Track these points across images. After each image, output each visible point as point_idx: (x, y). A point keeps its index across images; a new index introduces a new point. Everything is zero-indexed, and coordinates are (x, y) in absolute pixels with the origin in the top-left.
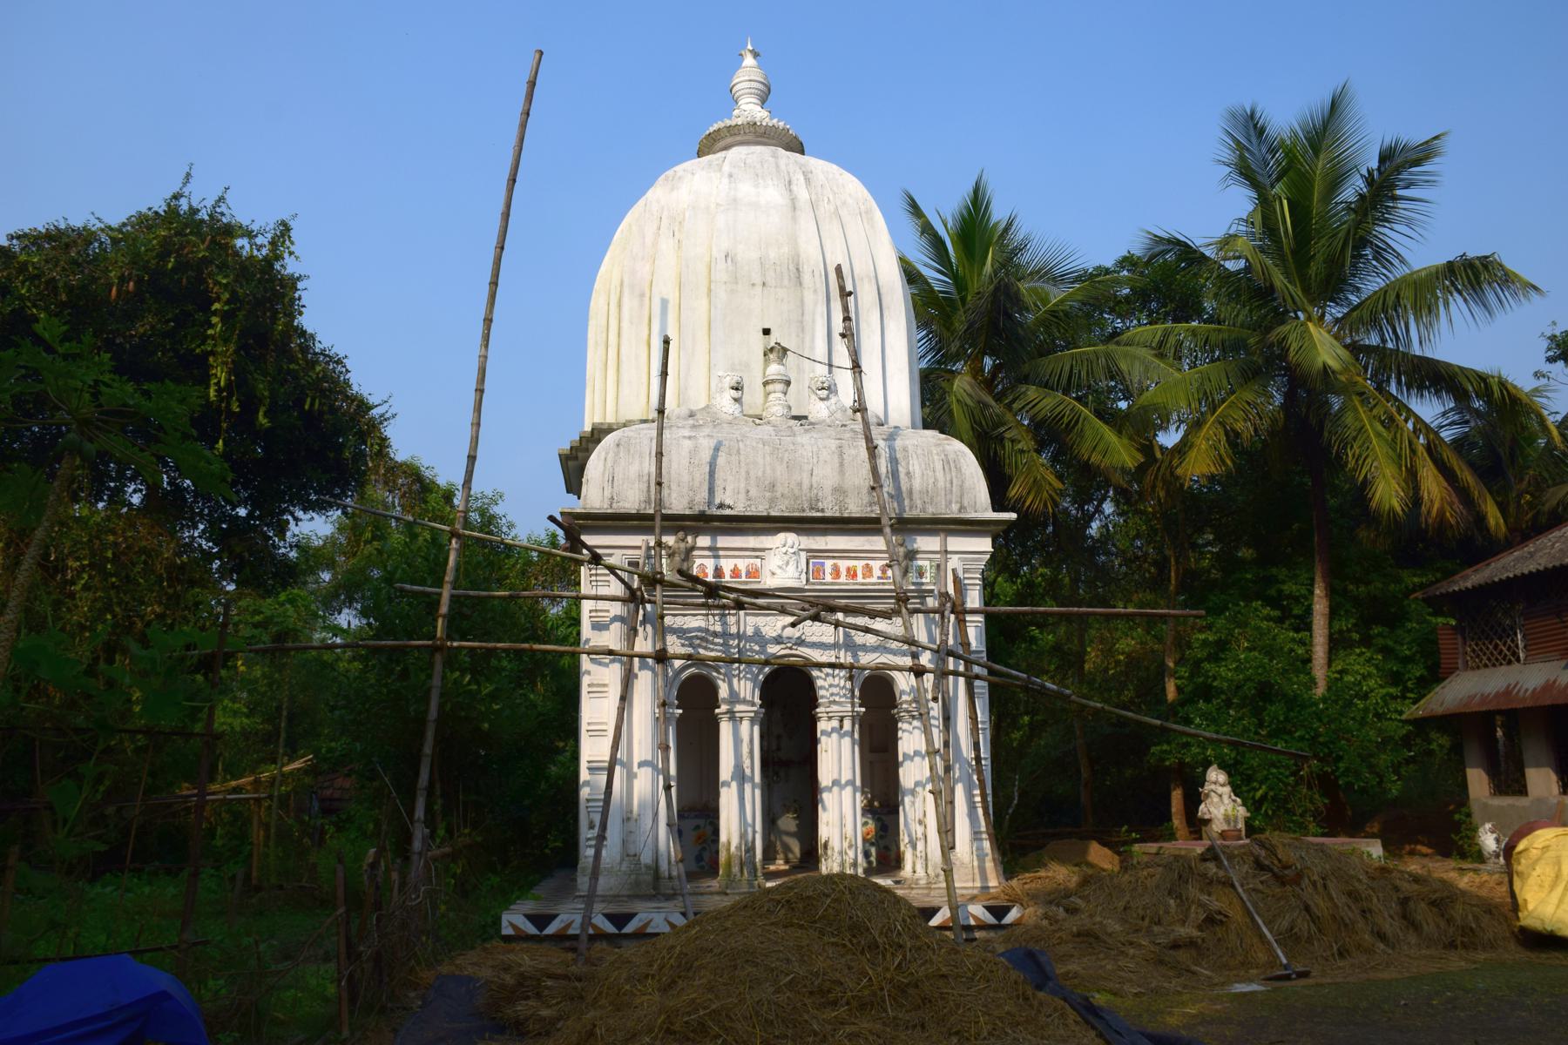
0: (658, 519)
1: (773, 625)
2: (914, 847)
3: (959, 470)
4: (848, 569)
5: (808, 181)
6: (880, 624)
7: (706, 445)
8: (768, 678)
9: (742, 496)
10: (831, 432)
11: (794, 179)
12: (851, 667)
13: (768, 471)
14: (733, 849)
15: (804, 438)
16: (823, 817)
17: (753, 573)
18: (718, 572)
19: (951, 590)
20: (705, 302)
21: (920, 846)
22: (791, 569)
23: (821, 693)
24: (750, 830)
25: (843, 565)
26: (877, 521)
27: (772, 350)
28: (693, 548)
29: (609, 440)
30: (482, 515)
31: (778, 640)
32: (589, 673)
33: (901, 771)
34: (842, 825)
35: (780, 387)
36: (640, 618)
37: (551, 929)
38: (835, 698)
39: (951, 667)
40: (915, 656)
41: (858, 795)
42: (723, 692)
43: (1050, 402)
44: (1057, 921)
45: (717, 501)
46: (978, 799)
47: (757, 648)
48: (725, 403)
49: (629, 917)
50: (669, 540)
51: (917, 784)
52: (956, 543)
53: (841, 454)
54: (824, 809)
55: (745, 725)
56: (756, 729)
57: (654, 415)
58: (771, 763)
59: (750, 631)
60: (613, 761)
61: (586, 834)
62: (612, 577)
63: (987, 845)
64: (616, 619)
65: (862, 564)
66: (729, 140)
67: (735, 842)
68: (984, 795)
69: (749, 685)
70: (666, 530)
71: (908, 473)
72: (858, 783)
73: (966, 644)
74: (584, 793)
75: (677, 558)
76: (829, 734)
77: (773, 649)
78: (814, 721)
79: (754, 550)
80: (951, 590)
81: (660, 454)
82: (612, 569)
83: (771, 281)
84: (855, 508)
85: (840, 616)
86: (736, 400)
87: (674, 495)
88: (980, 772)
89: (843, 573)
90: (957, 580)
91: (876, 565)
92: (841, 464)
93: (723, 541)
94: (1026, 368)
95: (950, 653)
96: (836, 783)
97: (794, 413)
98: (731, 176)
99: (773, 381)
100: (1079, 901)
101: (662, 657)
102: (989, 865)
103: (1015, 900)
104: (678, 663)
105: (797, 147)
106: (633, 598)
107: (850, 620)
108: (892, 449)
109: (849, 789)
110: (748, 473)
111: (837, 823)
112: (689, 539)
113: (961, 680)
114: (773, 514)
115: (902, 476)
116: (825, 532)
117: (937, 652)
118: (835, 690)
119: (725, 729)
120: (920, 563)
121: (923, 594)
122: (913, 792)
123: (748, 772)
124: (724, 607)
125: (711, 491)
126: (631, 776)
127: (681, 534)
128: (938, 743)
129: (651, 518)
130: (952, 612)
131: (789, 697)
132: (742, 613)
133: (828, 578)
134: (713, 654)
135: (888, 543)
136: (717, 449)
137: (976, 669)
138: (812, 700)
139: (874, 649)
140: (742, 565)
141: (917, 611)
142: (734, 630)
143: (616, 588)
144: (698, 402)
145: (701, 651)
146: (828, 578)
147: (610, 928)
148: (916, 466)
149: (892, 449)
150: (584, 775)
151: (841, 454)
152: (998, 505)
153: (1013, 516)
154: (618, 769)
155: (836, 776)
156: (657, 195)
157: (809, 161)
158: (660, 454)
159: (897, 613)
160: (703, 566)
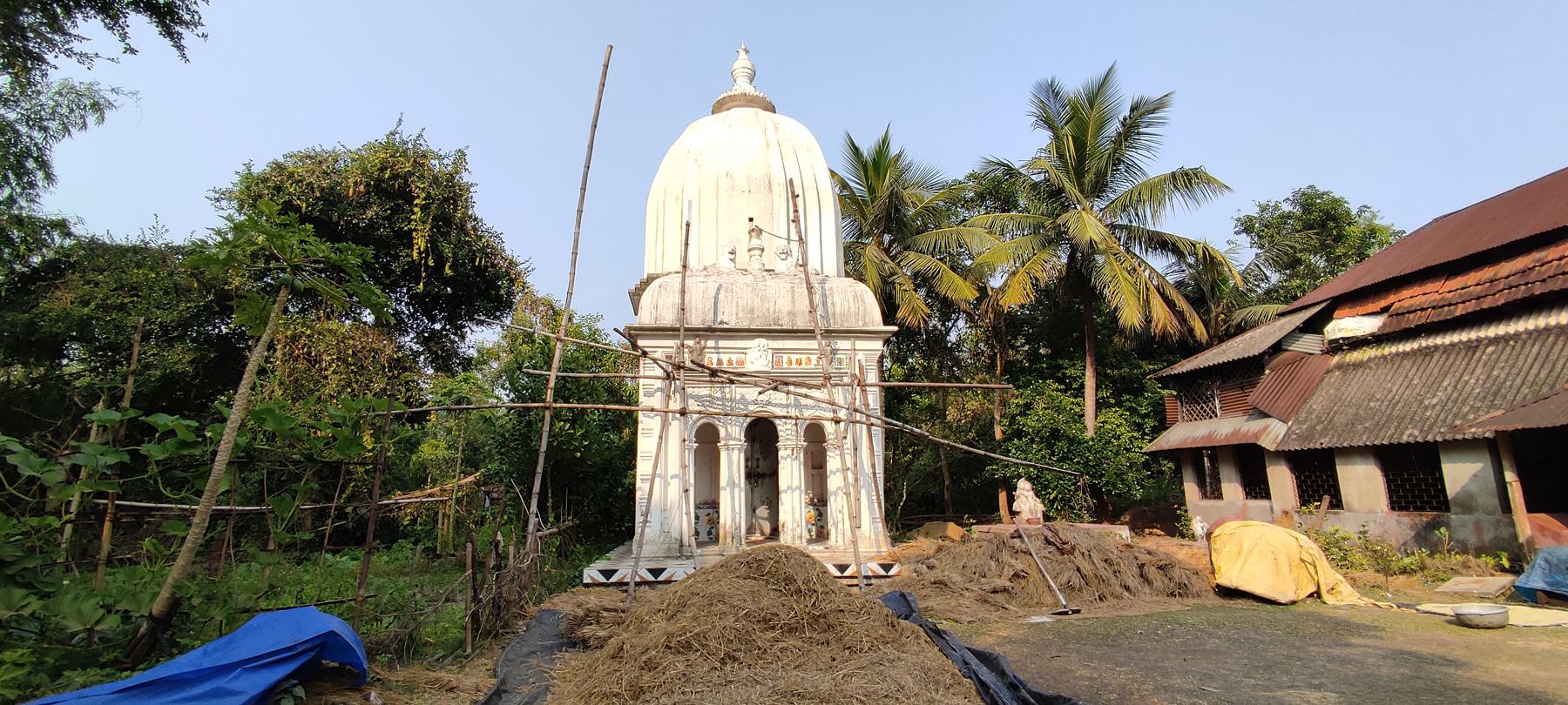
1: (751, 393)
6: (815, 393)
7: (713, 287)
17: (741, 363)
18: (720, 362)
25: (794, 357)
29: (656, 283)
31: (755, 402)
37: (614, 579)
38: (789, 441)
42: (722, 433)
48: (725, 263)
49: (662, 570)
50: (690, 343)
52: (860, 344)
58: (750, 475)
61: (639, 519)
63: (880, 525)
64: (658, 390)
65: (803, 356)
67: (729, 523)
70: (686, 337)
74: (638, 494)
77: (752, 408)
78: (777, 450)
81: (683, 292)
82: (655, 360)
84: (801, 324)
85: (792, 388)
91: (814, 358)
93: (722, 343)
94: (909, 241)
95: (856, 410)
96: (789, 488)
101: (683, 413)
102: (881, 538)
104: (695, 416)
106: (668, 377)
107: (799, 390)
116: (783, 338)
119: (723, 455)
121: (841, 375)
122: (836, 494)
125: (715, 313)
126: (666, 484)
128: (849, 463)
131: (762, 434)
138: (776, 438)
140: (734, 357)
147: (651, 578)
148: (837, 299)
152: (886, 323)
153: (896, 328)
154: (657, 480)
158: (683, 292)
160: (711, 359)
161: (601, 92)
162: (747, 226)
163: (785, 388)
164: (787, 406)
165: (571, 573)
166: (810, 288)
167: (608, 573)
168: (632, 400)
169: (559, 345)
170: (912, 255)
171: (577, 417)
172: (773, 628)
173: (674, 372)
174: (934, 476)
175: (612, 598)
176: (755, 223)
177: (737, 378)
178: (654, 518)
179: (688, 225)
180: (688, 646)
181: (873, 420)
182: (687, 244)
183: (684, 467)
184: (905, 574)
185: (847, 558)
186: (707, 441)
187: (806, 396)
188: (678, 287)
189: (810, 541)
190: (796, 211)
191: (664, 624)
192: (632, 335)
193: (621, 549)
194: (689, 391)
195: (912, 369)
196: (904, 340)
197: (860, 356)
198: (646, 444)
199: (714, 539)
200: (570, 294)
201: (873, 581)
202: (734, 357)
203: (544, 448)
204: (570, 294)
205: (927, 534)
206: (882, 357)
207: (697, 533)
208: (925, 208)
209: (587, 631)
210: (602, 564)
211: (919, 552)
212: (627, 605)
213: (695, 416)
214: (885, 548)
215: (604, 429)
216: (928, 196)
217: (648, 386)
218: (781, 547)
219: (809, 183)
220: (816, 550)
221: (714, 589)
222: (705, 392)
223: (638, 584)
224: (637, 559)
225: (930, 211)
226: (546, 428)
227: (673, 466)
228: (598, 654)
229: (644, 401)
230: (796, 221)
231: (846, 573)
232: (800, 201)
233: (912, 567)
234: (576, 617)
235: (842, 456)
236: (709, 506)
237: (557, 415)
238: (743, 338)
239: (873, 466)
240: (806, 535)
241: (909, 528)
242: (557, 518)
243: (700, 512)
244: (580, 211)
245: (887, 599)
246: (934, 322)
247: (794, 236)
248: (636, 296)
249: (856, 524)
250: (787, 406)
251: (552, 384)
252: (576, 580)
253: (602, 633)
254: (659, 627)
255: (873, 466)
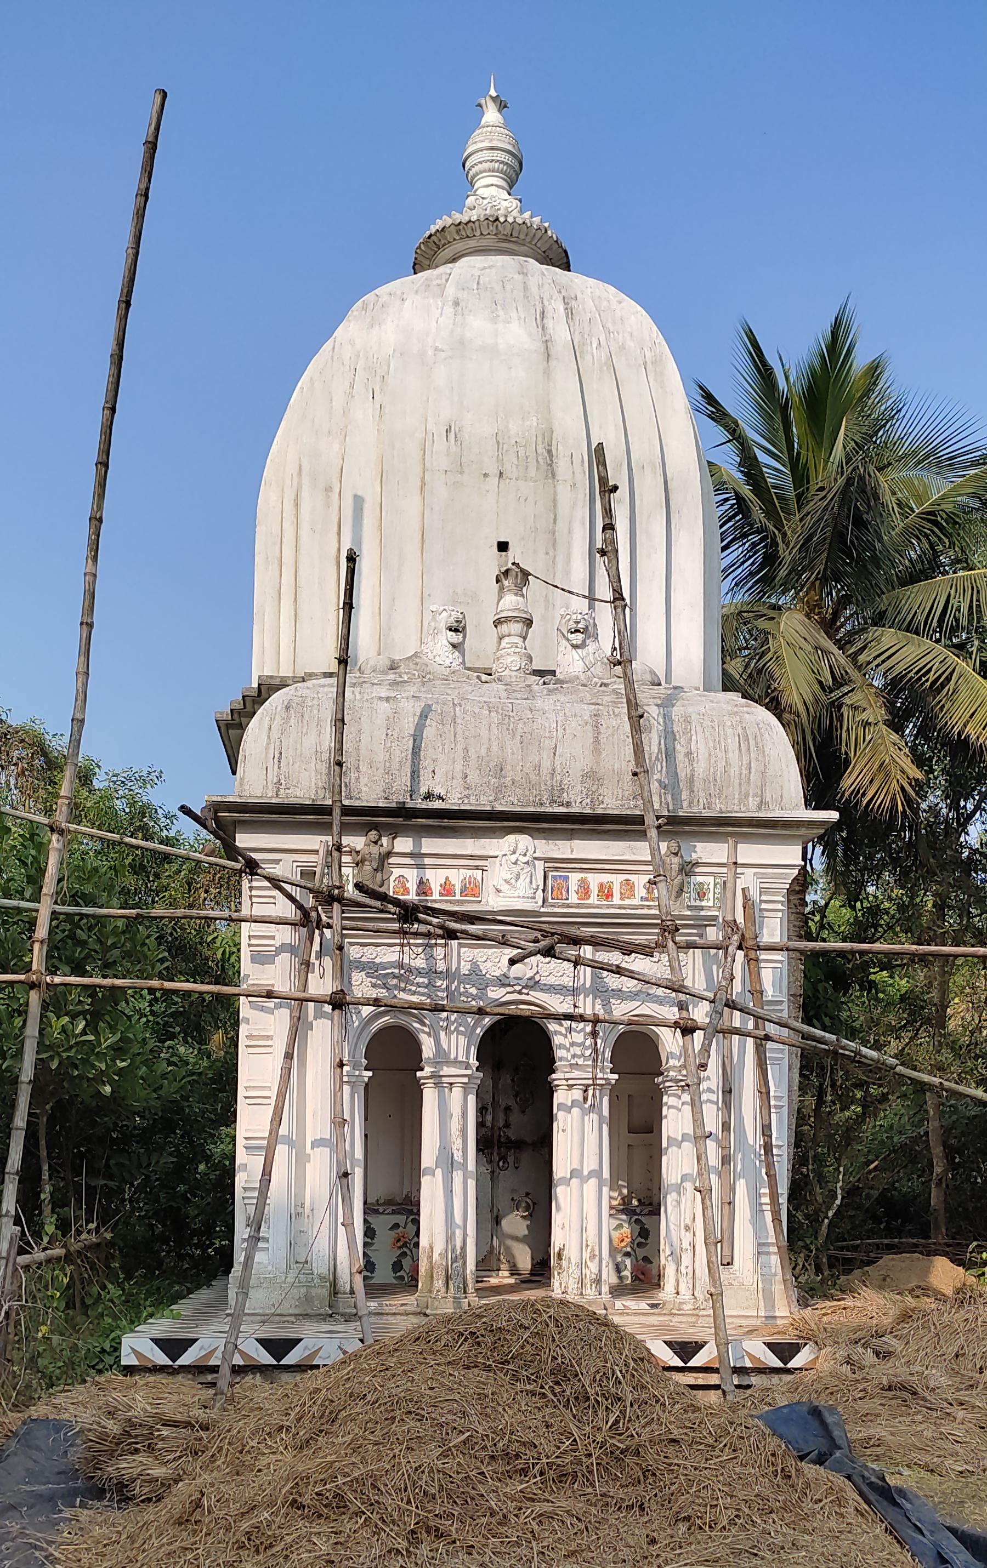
0: (337, 812)
1: (494, 961)
2: (678, 1263)
3: (761, 749)
4: (601, 886)
5: (570, 313)
6: (638, 963)
7: (410, 710)
8: (490, 1033)
9: (458, 783)
10: (585, 693)
11: (549, 310)
12: (596, 1021)
13: (495, 748)
14: (436, 1256)
15: (548, 703)
16: (557, 1219)
17: (471, 889)
19: (740, 919)
20: (417, 499)
21: (686, 1259)
22: (523, 883)
23: (559, 1053)
24: (458, 1233)
25: (594, 880)
26: (640, 820)
27: (506, 573)
28: (389, 854)
29: (276, 700)
30: (132, 804)
31: (503, 981)
32: (247, 1021)
33: (664, 1159)
34: (583, 1229)
35: (517, 627)
36: (316, 947)
37: (186, 1359)
38: (577, 1063)
39: (737, 1023)
40: (682, 1007)
41: (605, 1190)
42: (428, 1049)
43: (910, 652)
44: (862, 1368)
45: (423, 790)
46: (766, 1200)
47: (474, 991)
48: (440, 651)
50: (357, 842)
51: (684, 1178)
52: (749, 852)
53: (597, 726)
54: (558, 1209)
55: (457, 1092)
56: (472, 1099)
57: (334, 667)
58: (488, 1144)
59: (465, 970)
60: (274, 1138)
61: (241, 1232)
62: (276, 893)
63: (775, 1260)
64: (283, 948)
65: (616, 879)
66: (459, 246)
67: (439, 1248)
68: (774, 1195)
69: (463, 1040)
70: (346, 828)
71: (689, 754)
72: (606, 1174)
73: (757, 992)
75: (367, 867)
76: (568, 1110)
77: (496, 993)
79: (472, 857)
80: (740, 919)
81: (340, 722)
82: (275, 883)
83: (510, 470)
84: (612, 804)
85: (587, 951)
86: (454, 646)
87: (364, 780)
88: (770, 1166)
89: (594, 890)
90: (748, 904)
91: (640, 881)
92: (596, 740)
93: (430, 845)
94: (883, 602)
95: (731, 1005)
96: (574, 1173)
97: (535, 667)
98: (456, 304)
99: (507, 620)
100: (894, 1342)
101: (339, 1002)
103: (809, 1337)
105: (560, 259)
106: (306, 921)
107: (604, 956)
108: (667, 718)
109: (593, 1182)
110: (466, 750)
111: (576, 1226)
112: (384, 840)
113: (750, 1041)
114: (499, 808)
115: (680, 757)
116: (571, 835)
117: (712, 1002)
118: (578, 1051)
119: (430, 1096)
120: (699, 879)
121: (702, 923)
122: (679, 1189)
123: (458, 1156)
124: (428, 935)
125: (415, 774)
126: (302, 1159)
127: (373, 834)
128: (712, 1122)
129: (326, 811)
130: (740, 948)
131: (516, 1054)
132: (454, 943)
133: (574, 898)
134: (415, 999)
135: (654, 851)
136: (424, 716)
137: (772, 1029)
139: (634, 996)
140: (456, 878)
141: (691, 946)
142: (441, 966)
143: (286, 910)
144: (404, 646)
145: (402, 995)
146: (574, 898)
148: (700, 745)
149: (667, 718)
150: (241, 1156)
151: (597, 726)
153: (834, 816)
154: (281, 1151)
155: (576, 1165)
156: (350, 332)
157: (575, 280)
158: (340, 722)
159: (661, 946)
160: (403, 881)
161: (140, 214)
162: (492, 563)
163: (572, 952)
164: (574, 992)
165: (95, 1344)
166: (636, 719)
167: (173, 1347)
168: (226, 971)
169: (55, 842)
170: (888, 637)
171: (102, 1007)
172: (524, 1472)
173: (318, 908)
174: (911, 1155)
175: (182, 1397)
176: (514, 554)
177: (457, 925)
178: (275, 1233)
179: (352, 559)
180: (340, 1503)
181: (772, 1029)
182: (349, 606)
183: (339, 1122)
184: (825, 1366)
185: (701, 1330)
186: (392, 1067)
187: (618, 970)
188: (328, 713)
189: (618, 1291)
190: (609, 527)
191: (288, 1456)
192: (224, 820)
193: (203, 1295)
194: (354, 952)
195: (874, 911)
196: (857, 839)
197: (747, 879)
198: (257, 1071)
199: (406, 1278)
200: (79, 722)
201: (754, 1380)
202: (456, 878)
203: (27, 1072)
204: (79, 722)
205: (883, 1284)
206: (803, 881)
207: (369, 1266)
208: (930, 517)
209: (128, 1466)
210: (162, 1326)
211: (857, 1320)
212: (213, 1414)
213: (366, 1011)
214: (784, 1309)
215: (164, 1034)
216: (938, 488)
217: (263, 941)
218: (548, 1303)
219: (643, 450)
220: (630, 1314)
221: (398, 1387)
222: (388, 954)
223: (238, 1371)
224: (237, 1319)
225: (941, 525)
226: (32, 1030)
227: (317, 1123)
228: (150, 1512)
229: (252, 974)
230: (608, 551)
231: (695, 1362)
232: (620, 504)
233: (841, 1354)
234: (103, 1437)
235: (696, 1106)
236: (394, 1210)
237: (56, 1001)
238: (477, 833)
239: (766, 1130)
240: (609, 1277)
241: (848, 1266)
242: (63, 1226)
243: (375, 1221)
244: (97, 521)
245: (778, 1421)
246: (934, 798)
247: (604, 591)
248: (232, 729)
249: (720, 1247)
250: (574, 992)
251: (42, 931)
252: (105, 1359)
253: (158, 1471)
254: (278, 1465)
255: (766, 1130)
